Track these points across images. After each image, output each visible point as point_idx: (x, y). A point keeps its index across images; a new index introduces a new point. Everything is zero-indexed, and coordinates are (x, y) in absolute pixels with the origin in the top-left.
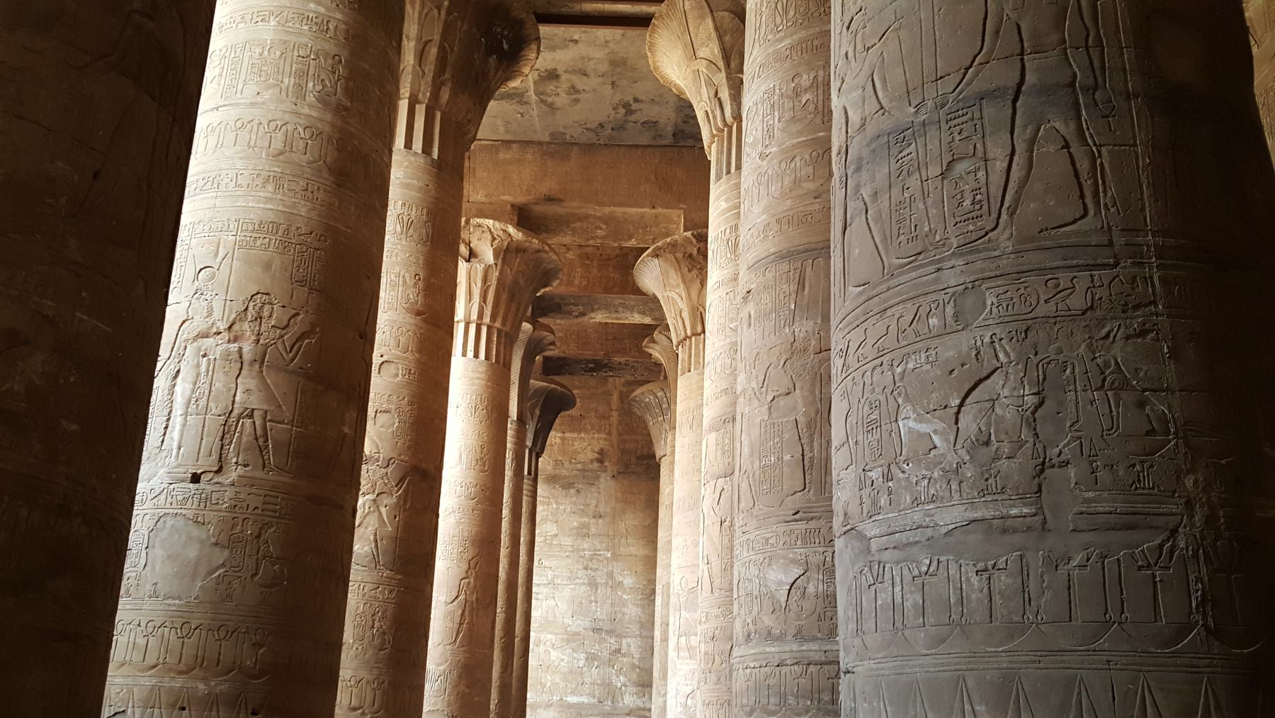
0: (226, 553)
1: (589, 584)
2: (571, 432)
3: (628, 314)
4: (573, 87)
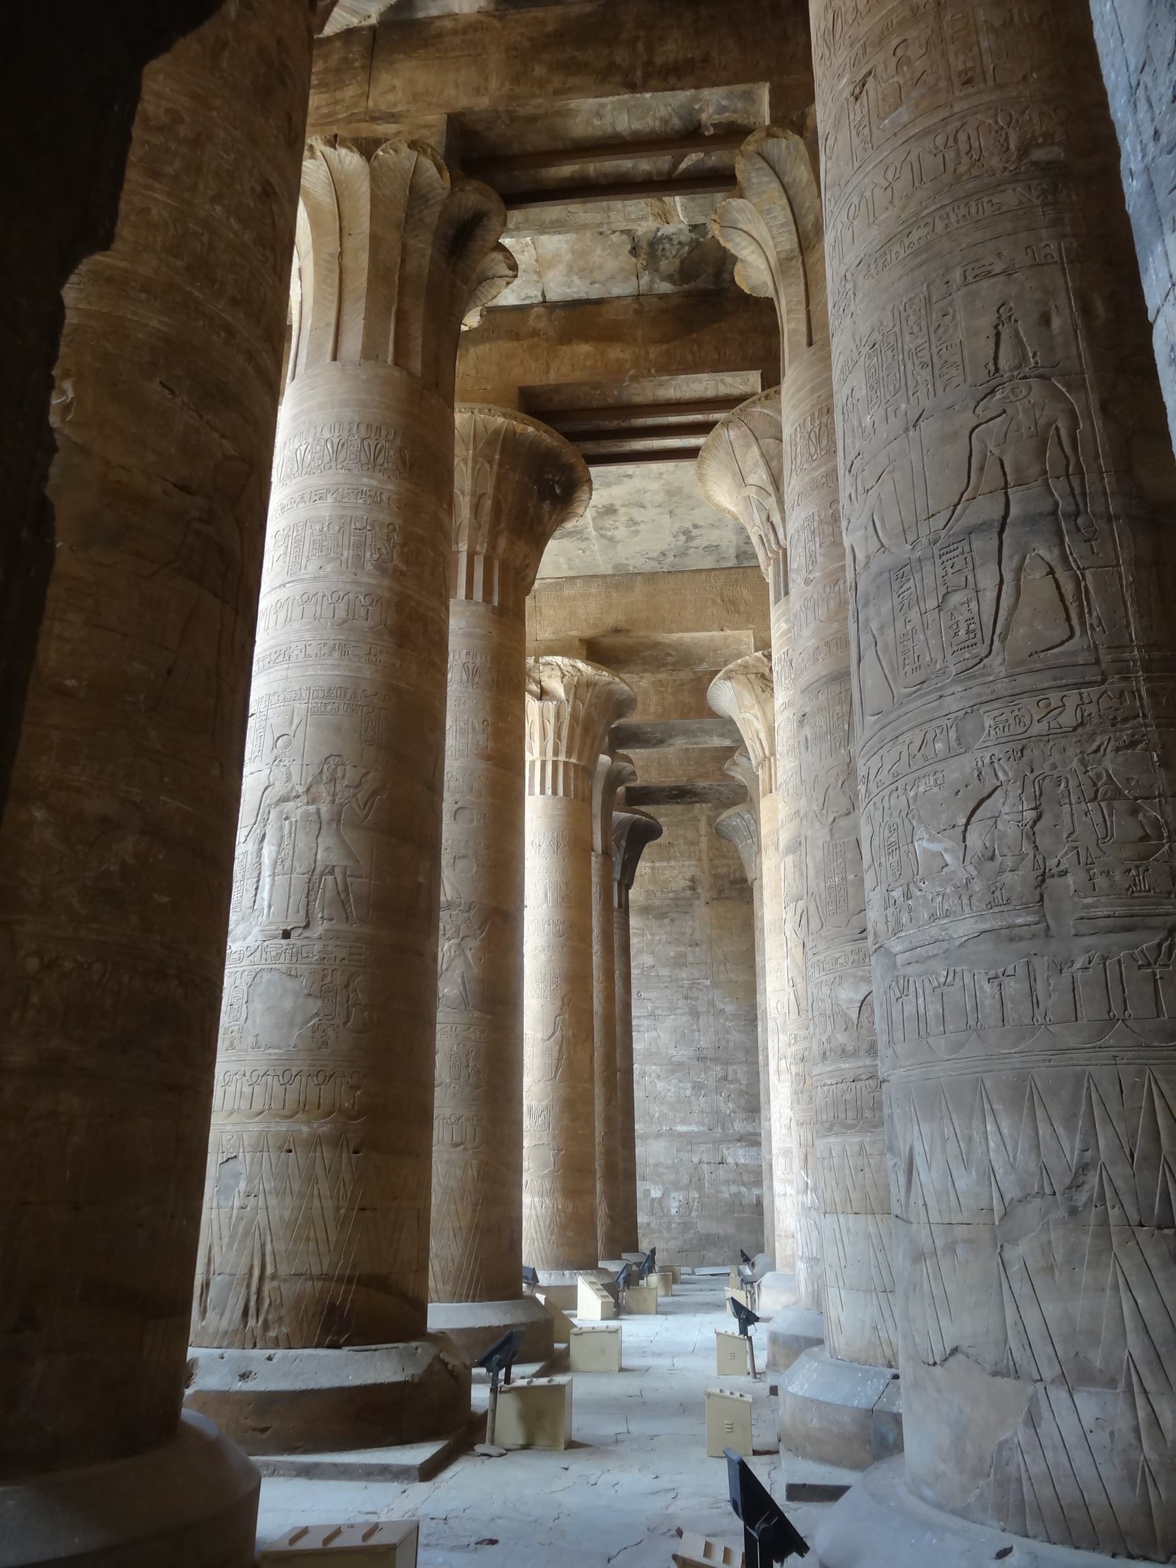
0: (319, 1003)
3: (707, 738)
4: (631, 519)
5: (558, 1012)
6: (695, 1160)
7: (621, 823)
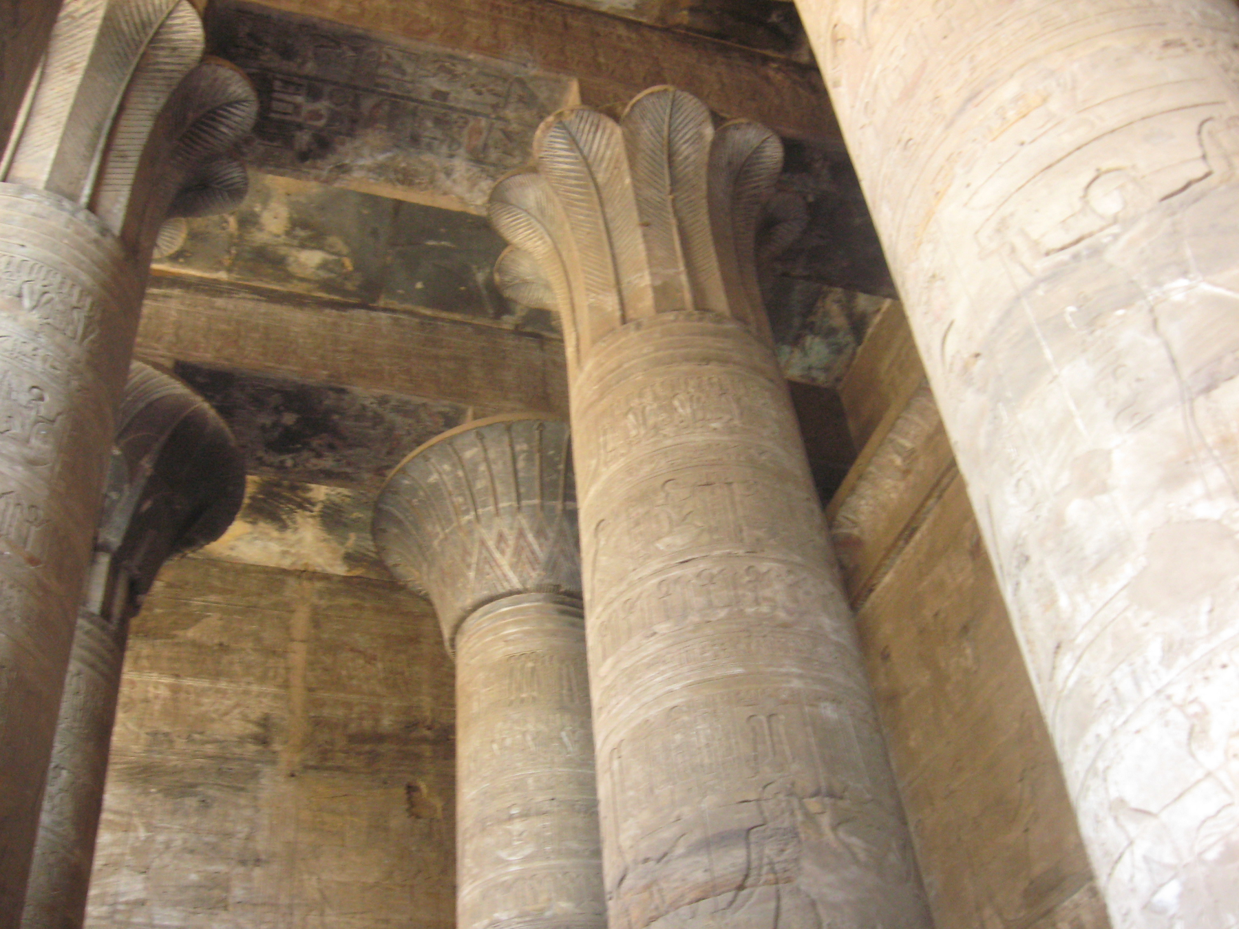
2: (196, 675)
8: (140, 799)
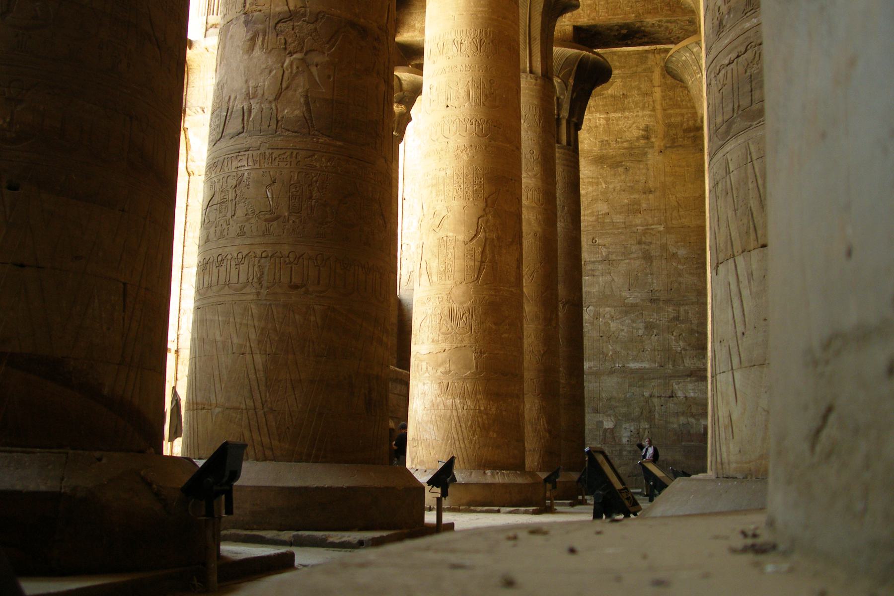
1: (644, 258)
2: (615, 112)
5: (481, 213)
6: (647, 394)
7: (568, 60)
8: (601, 171)
